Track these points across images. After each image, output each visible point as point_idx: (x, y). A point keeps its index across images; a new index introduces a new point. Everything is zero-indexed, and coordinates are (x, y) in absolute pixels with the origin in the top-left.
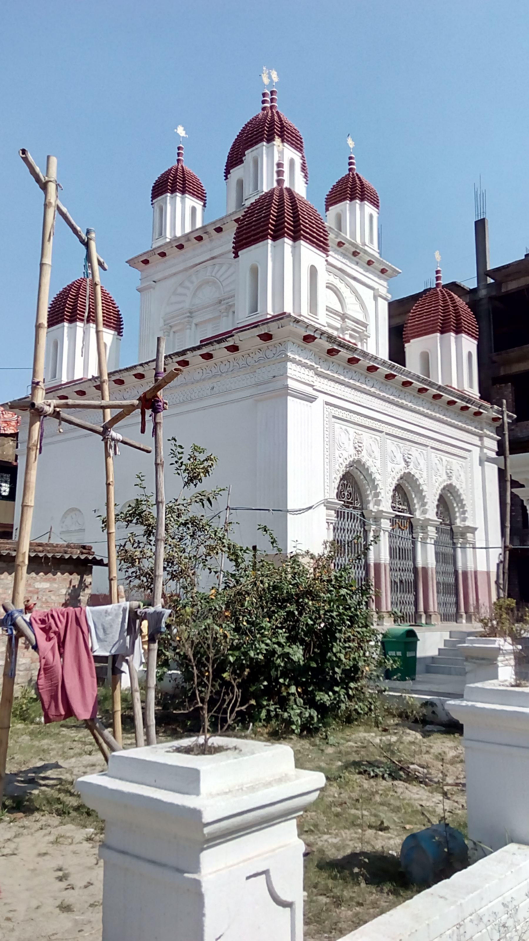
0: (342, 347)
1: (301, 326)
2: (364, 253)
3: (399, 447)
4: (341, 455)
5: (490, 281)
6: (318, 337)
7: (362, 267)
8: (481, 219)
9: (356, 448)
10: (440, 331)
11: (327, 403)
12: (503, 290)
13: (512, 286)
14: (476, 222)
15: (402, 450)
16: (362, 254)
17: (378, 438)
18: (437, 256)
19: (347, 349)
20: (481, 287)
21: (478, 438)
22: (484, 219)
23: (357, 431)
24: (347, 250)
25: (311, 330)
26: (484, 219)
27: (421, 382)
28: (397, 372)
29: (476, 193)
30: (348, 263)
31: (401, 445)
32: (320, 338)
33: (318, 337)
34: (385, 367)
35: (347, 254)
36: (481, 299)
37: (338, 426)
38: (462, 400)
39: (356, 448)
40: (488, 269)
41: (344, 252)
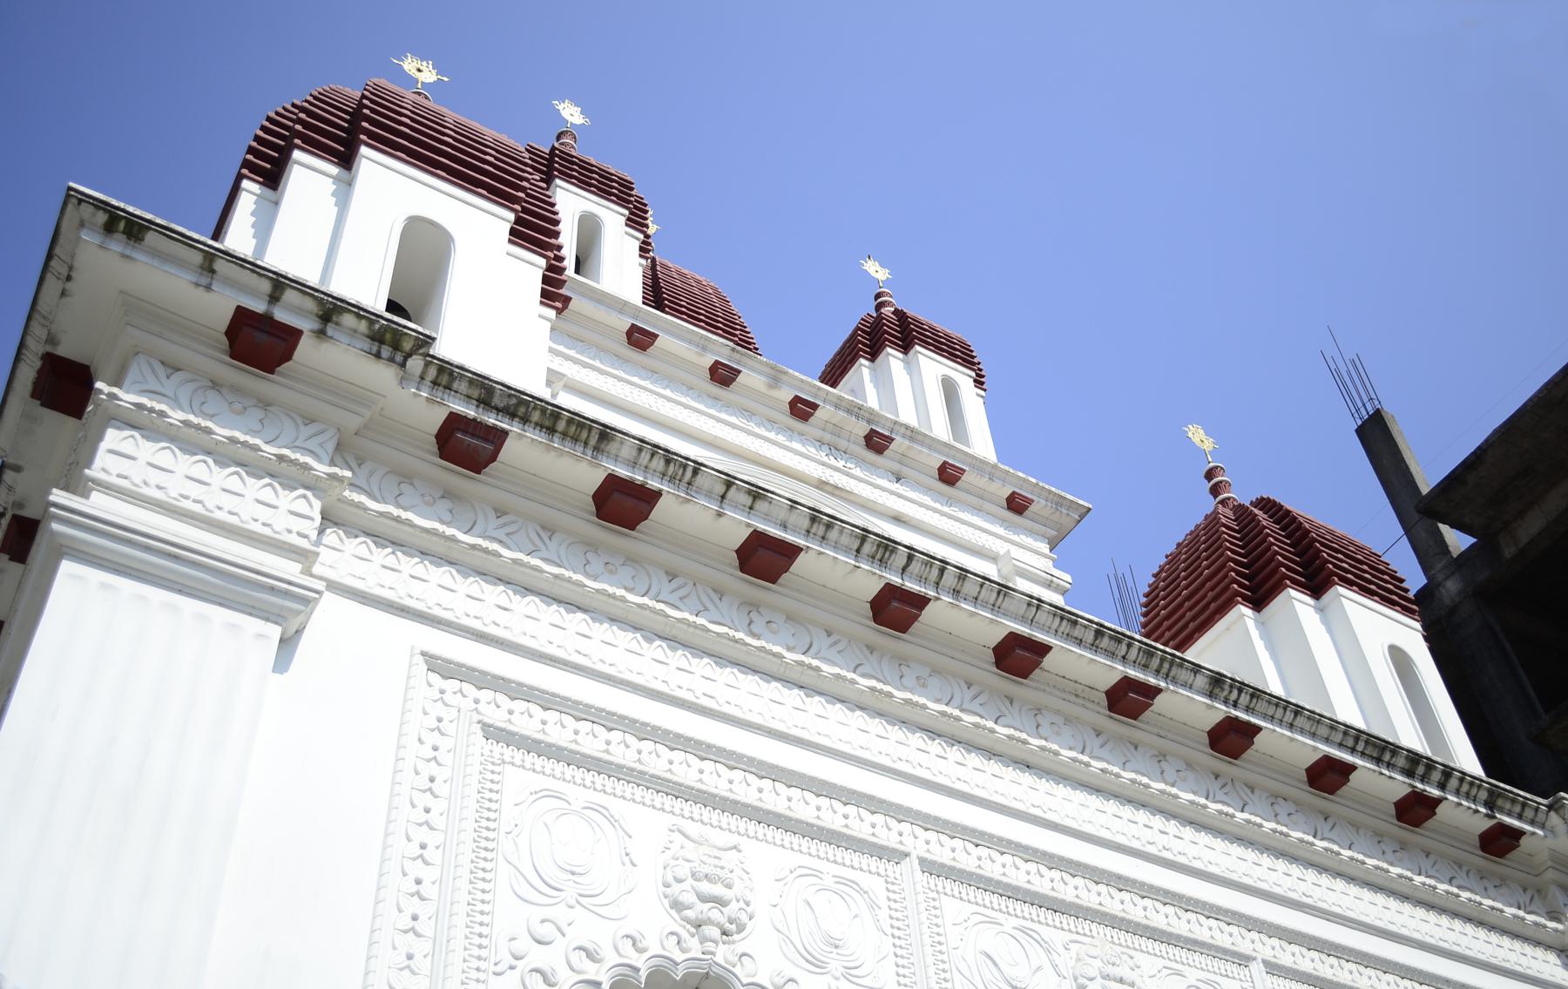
0: (513, 415)
1: (156, 254)
2: (911, 439)
3: (1041, 942)
4: (547, 931)
5: (1457, 541)
6: (306, 325)
7: (927, 490)
8: (1371, 417)
9: (677, 905)
10: (1246, 599)
11: (439, 666)
12: (1508, 552)
13: (1530, 527)
14: (1360, 431)
15: (1066, 961)
16: (898, 439)
17: (876, 886)
18: (1197, 434)
19: (551, 430)
20: (1440, 577)
21: (1552, 957)
22: (1378, 413)
23: (693, 829)
24: (837, 430)
25: (253, 293)
26: (1378, 413)
27: (1094, 647)
28: (921, 579)
29: (1336, 374)
30: (857, 472)
31: (1057, 938)
32: (321, 334)
33: (306, 325)
34: (836, 547)
35: (843, 444)
36: (1453, 610)
37: (521, 777)
38: (1378, 761)
39: (677, 905)
40: (1425, 490)
41: (827, 437)
